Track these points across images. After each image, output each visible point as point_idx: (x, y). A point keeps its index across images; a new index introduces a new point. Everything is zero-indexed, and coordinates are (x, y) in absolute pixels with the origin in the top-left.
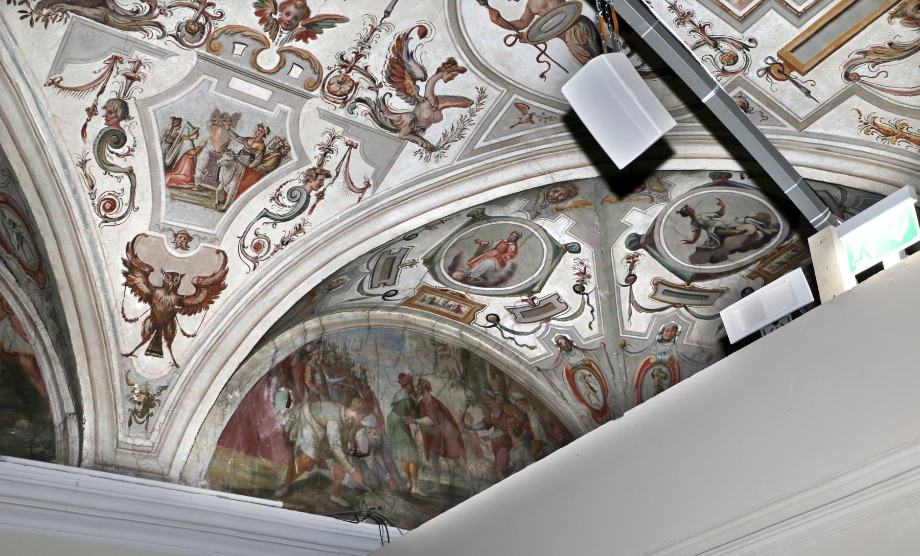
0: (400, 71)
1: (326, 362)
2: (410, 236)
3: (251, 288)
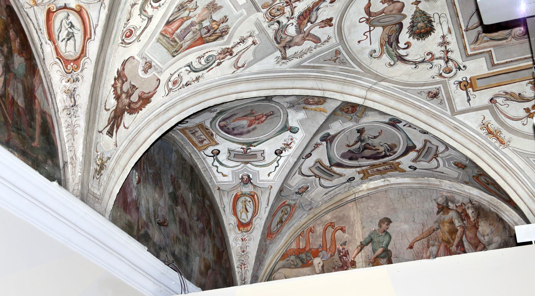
0: (306, 16)
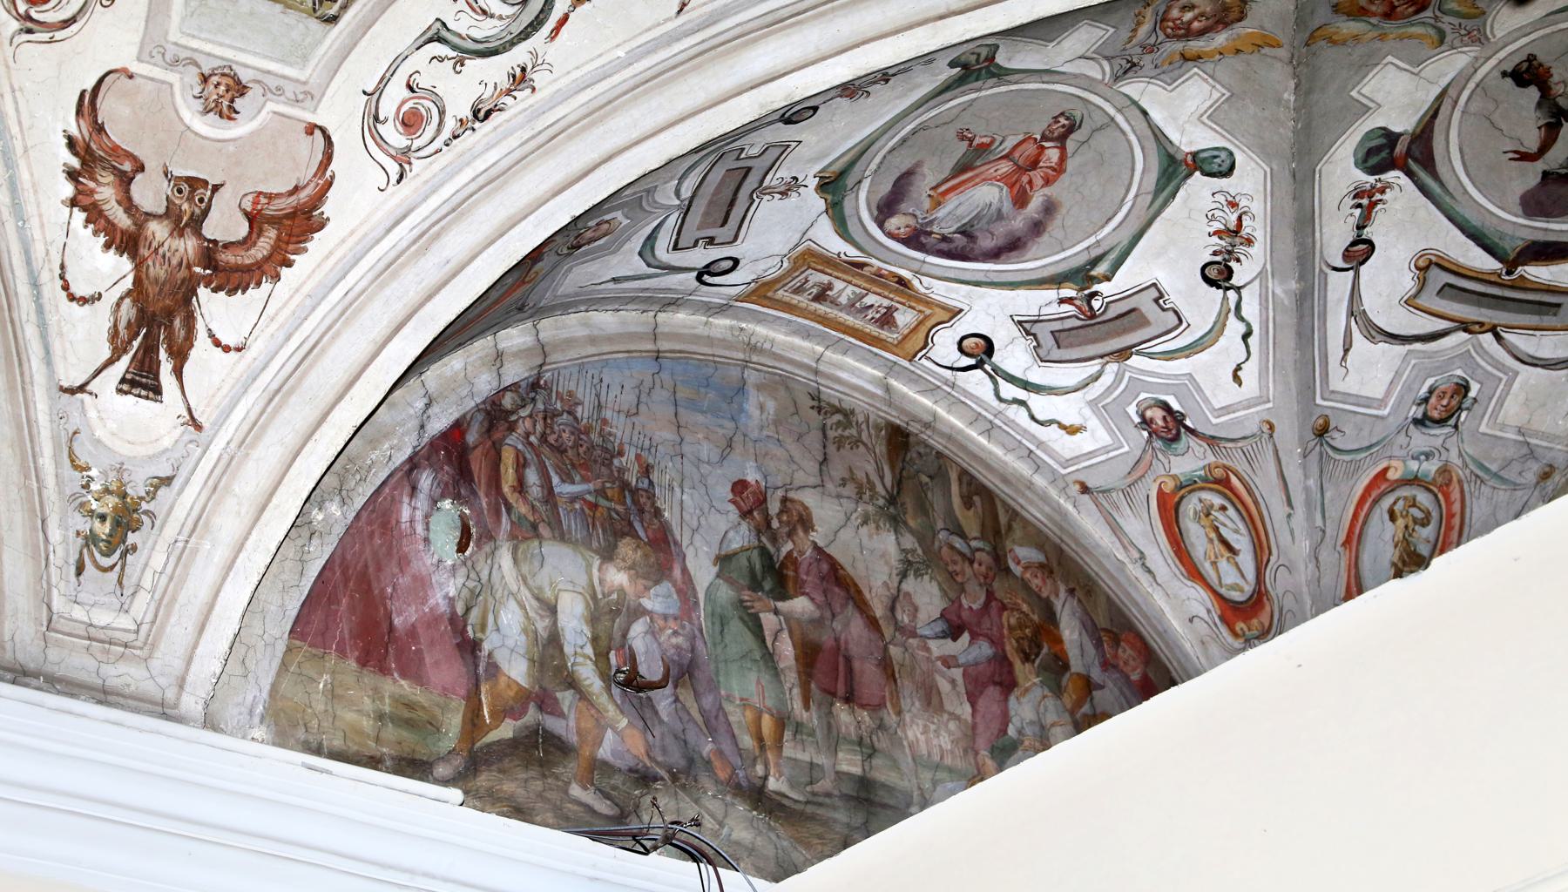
1: (552, 439)
3: (389, 231)
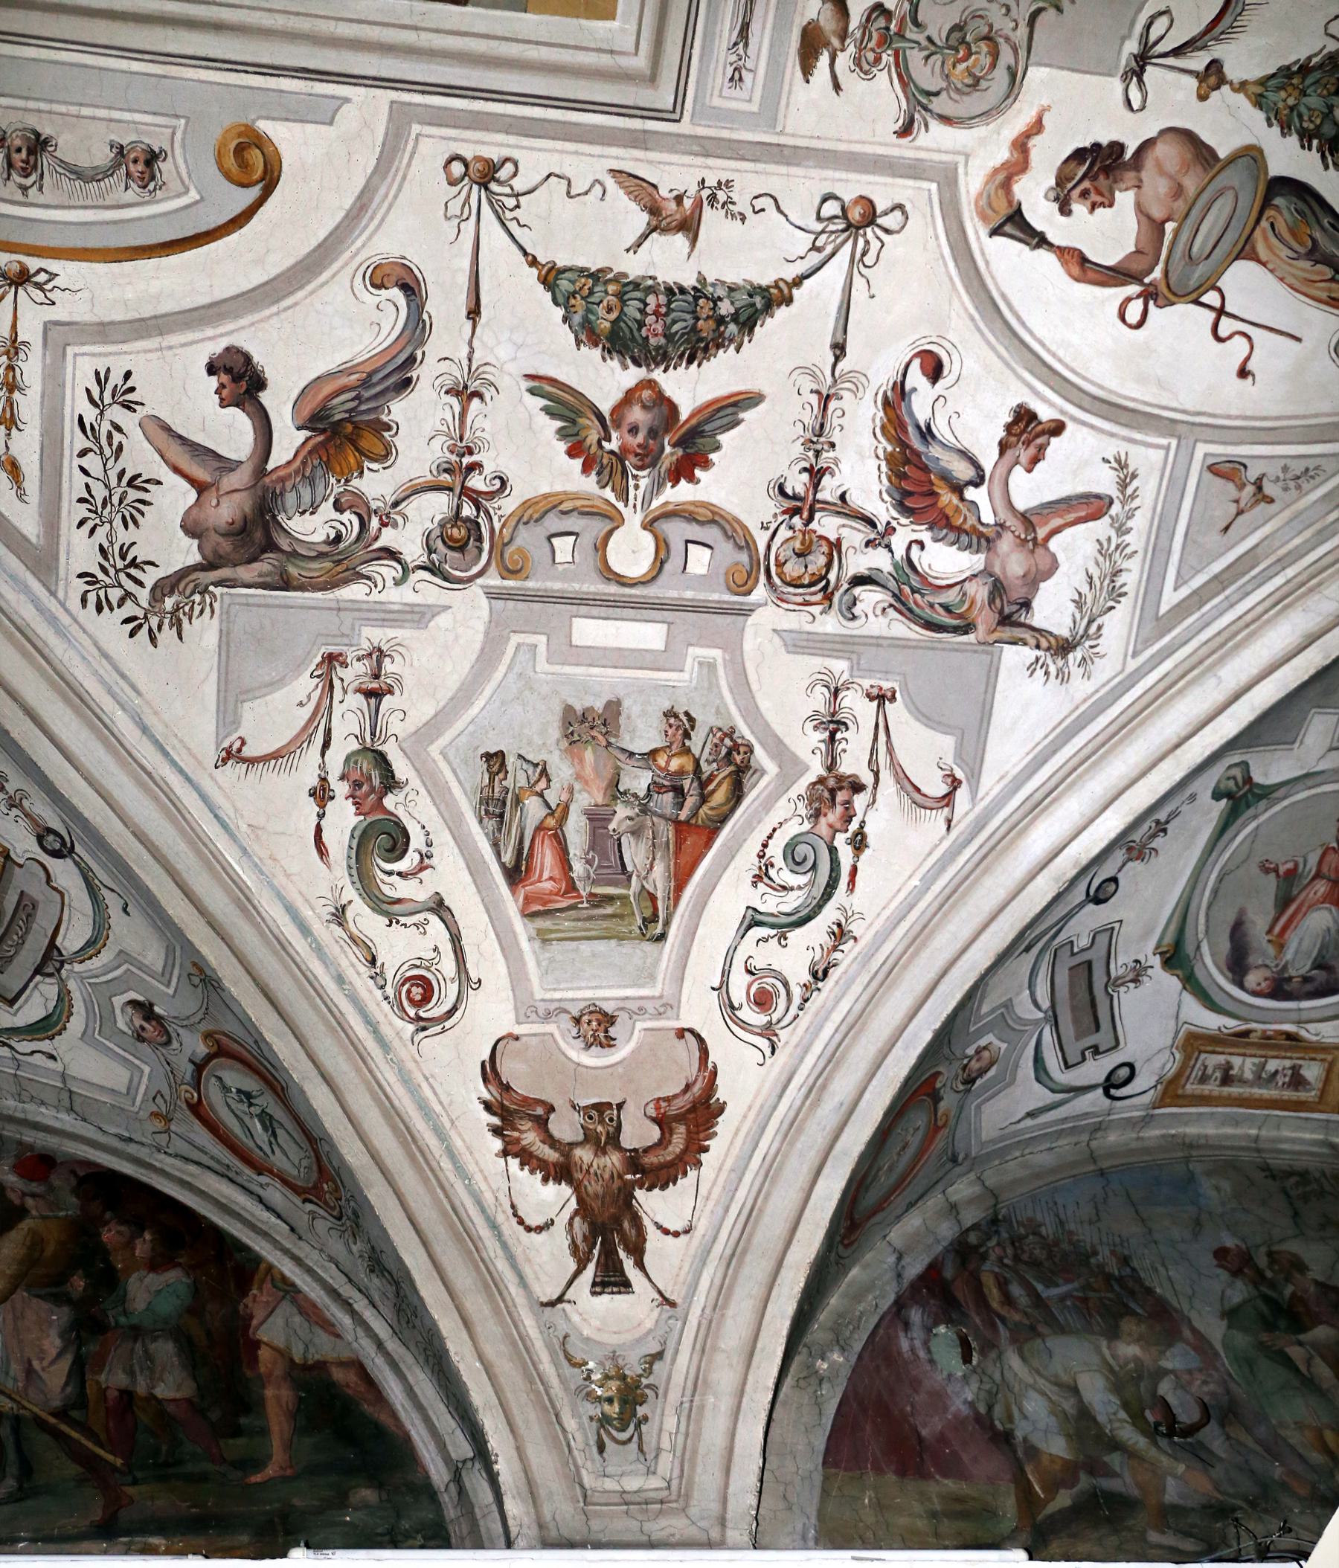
0: (919, 480)
2: (1096, 885)
3: (780, 1097)
